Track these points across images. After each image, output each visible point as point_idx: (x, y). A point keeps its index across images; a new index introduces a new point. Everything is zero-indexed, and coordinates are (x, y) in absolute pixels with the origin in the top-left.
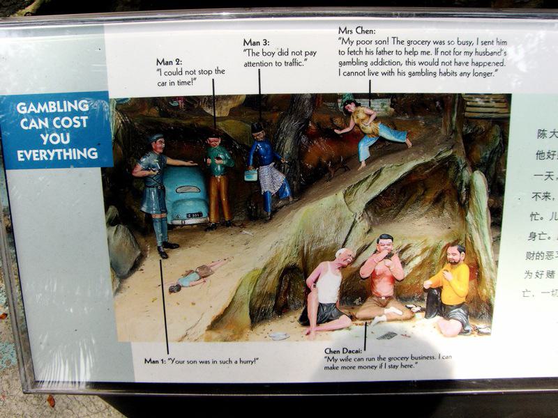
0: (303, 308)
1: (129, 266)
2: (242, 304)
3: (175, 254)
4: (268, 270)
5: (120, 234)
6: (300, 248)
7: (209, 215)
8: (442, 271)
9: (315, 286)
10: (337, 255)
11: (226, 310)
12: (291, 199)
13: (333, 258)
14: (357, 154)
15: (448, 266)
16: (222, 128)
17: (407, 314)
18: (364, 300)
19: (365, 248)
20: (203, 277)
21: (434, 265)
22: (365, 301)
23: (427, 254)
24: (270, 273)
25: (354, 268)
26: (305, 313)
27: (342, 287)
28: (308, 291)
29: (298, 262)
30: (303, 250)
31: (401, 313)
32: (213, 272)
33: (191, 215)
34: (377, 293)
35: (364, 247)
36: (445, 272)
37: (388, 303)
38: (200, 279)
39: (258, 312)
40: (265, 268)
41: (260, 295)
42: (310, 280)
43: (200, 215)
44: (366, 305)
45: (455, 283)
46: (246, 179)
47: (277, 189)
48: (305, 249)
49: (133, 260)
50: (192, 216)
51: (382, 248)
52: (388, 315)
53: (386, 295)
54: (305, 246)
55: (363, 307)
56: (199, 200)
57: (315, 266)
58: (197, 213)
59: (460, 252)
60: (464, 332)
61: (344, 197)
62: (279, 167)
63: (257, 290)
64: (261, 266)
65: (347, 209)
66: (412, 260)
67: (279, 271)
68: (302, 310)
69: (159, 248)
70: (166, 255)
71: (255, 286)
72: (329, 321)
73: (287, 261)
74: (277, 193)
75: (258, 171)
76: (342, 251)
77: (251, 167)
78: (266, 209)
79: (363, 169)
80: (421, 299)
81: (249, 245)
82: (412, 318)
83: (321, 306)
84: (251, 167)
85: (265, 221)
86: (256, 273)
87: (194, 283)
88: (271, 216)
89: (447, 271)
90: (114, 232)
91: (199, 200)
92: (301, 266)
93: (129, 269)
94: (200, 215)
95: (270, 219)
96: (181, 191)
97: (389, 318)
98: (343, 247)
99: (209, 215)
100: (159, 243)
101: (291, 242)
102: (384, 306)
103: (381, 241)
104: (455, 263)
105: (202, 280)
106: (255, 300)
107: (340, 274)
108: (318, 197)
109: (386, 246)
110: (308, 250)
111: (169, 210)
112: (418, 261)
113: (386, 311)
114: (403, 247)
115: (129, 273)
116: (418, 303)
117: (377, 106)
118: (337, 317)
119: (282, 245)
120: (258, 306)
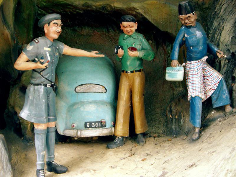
7: (114, 125)
16: (140, 11)
33: (91, 123)
43: (102, 125)
46: (168, 78)
47: (210, 94)
50: (91, 127)
56: (103, 103)
58: (98, 122)
62: (213, 62)
74: (209, 100)
75: (184, 67)
77: (175, 62)
78: (193, 119)
84: (175, 62)
91: (103, 103)
94: (102, 125)
95: (199, 138)
96: (82, 91)
99: (114, 125)
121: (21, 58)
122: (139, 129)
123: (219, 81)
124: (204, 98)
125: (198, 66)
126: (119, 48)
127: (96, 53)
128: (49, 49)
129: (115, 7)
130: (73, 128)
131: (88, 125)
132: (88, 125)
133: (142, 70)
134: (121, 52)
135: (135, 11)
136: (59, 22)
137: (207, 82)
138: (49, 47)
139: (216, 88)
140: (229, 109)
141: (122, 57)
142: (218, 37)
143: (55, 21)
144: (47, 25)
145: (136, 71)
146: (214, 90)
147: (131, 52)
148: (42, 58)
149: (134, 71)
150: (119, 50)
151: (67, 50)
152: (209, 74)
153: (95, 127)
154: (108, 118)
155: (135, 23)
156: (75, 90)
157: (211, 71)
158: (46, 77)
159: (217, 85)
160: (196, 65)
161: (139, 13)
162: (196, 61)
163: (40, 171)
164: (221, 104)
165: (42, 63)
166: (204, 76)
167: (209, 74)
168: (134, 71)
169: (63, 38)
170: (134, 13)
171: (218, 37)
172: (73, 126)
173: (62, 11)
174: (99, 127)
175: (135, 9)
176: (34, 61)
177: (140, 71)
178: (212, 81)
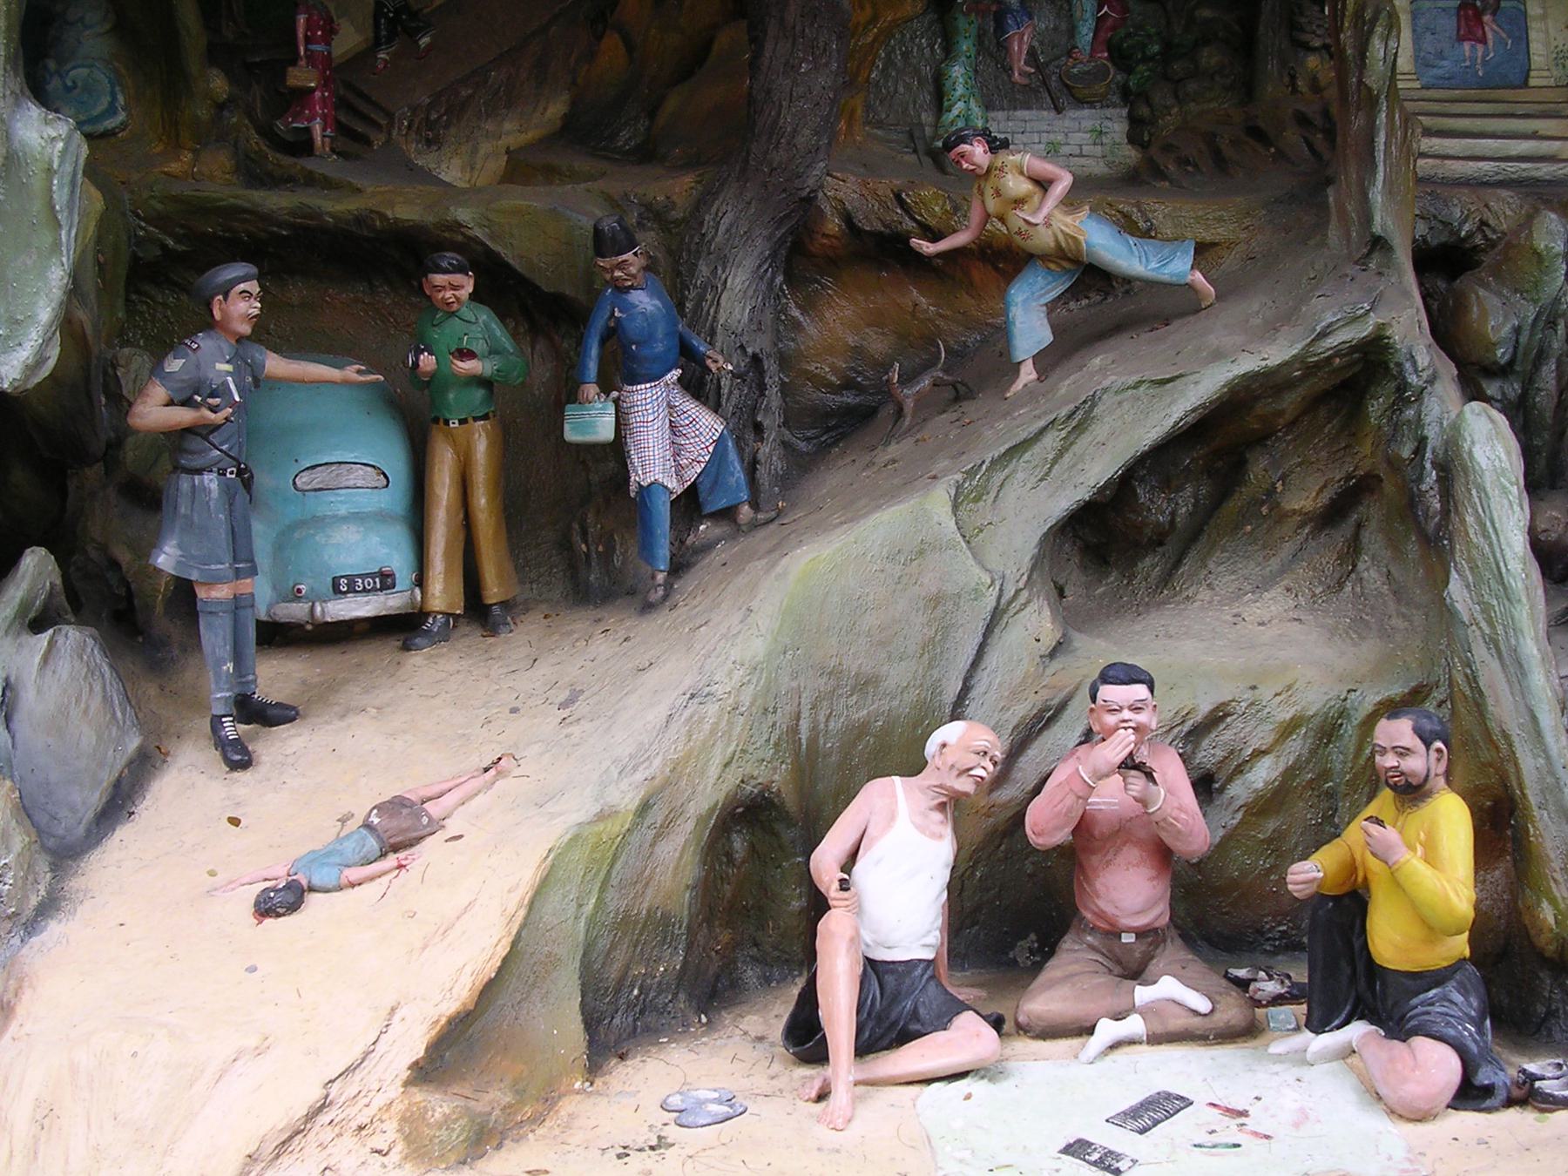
0: (801, 982)
1: (95, 799)
2: (552, 962)
3: (274, 746)
4: (657, 815)
5: (65, 666)
6: (782, 719)
7: (421, 581)
8: (1359, 823)
9: (844, 885)
10: (931, 746)
11: (489, 991)
12: (746, 511)
13: (913, 766)
14: (1001, 333)
15: (1384, 802)
16: (478, 233)
17: (1232, 1012)
18: (1047, 950)
19: (1045, 719)
20: (396, 848)
21: (1330, 795)
22: (1051, 953)
23: (1296, 746)
24: (662, 831)
25: (1004, 806)
26: (808, 1002)
27: (957, 886)
28: (819, 905)
29: (777, 776)
30: (794, 730)
31: (1201, 1004)
32: (436, 826)
33: (351, 580)
34: (1101, 915)
35: (1039, 716)
36: (1374, 829)
37: (1147, 959)
38: (383, 855)
39: (618, 991)
40: (645, 808)
41: (625, 922)
42: (826, 859)
43: (386, 581)
44: (1054, 969)
45: (1413, 864)
46: (571, 435)
47: (692, 474)
48: (804, 726)
49: (107, 777)
50: (352, 589)
51: (1111, 720)
52: (1147, 1012)
53: (1141, 921)
54: (805, 714)
55: (1043, 977)
56: (381, 517)
57: (844, 796)
58: (372, 575)
59: (1428, 745)
60: (1470, 1094)
61: (955, 507)
62: (698, 386)
63: (615, 902)
64: (626, 797)
65: (971, 561)
66: (1239, 770)
67: (702, 820)
68: (796, 991)
69: (216, 722)
70: (245, 751)
71: (602, 890)
72: (904, 1037)
73: (732, 779)
74: (692, 492)
75: (616, 401)
76: (951, 732)
77: (591, 390)
78: (647, 550)
79: (1030, 394)
80: (1290, 946)
81: (580, 707)
82: (1247, 1032)
83: (873, 968)
84: (591, 390)
85: (648, 608)
86: (615, 827)
87: (354, 874)
88: (668, 586)
89: (1380, 822)
90: (37, 659)
91: (381, 517)
92: (790, 801)
93: (90, 815)
94: (386, 581)
95: (666, 597)
96: (315, 485)
97: (1158, 1029)
98: (955, 716)
99: (421, 581)
100: (220, 696)
101: (746, 698)
102: (1136, 972)
103: (1109, 692)
104: (1412, 792)
105: (391, 860)
106: (603, 944)
107: (948, 831)
108: (852, 511)
109: (1126, 714)
110: (814, 728)
111: (263, 559)
112: (1263, 774)
113: (1143, 994)
114: (1199, 717)
115: (88, 831)
116: (1282, 963)
117: (1077, 138)
118: (942, 1021)
119: (712, 709)
120: (613, 973)
121: (148, 395)
122: (493, 591)
123: (715, 438)
124: (675, 486)
125: (655, 397)
126: (422, 352)
127: (359, 372)
128: (229, 368)
129: (396, 219)
130: (297, 596)
131: (342, 586)
132: (342, 586)
133: (491, 415)
134: (427, 361)
135: (462, 234)
136: (253, 287)
137: (683, 442)
138: (228, 362)
139: (707, 458)
140: (746, 511)
141: (431, 377)
142: (712, 311)
143: (242, 286)
144: (220, 297)
145: (475, 419)
146: (703, 465)
147: (460, 364)
148: (213, 395)
149: (470, 420)
150: (422, 357)
151: (275, 364)
152: (687, 418)
153: (365, 590)
154: (400, 562)
155: (467, 274)
156: (294, 483)
157: (693, 411)
158: (224, 447)
159: (711, 449)
160: (649, 395)
161: (475, 240)
162: (648, 385)
163: (224, 720)
164: (722, 503)
165: (214, 409)
166: (672, 426)
167: (687, 418)
168: (470, 420)
169: (265, 333)
170: (460, 238)
171: (712, 311)
172: (299, 591)
173: (220, 228)
174: (374, 590)
175: (461, 225)
176: (187, 403)
177: (485, 417)
178: (697, 439)
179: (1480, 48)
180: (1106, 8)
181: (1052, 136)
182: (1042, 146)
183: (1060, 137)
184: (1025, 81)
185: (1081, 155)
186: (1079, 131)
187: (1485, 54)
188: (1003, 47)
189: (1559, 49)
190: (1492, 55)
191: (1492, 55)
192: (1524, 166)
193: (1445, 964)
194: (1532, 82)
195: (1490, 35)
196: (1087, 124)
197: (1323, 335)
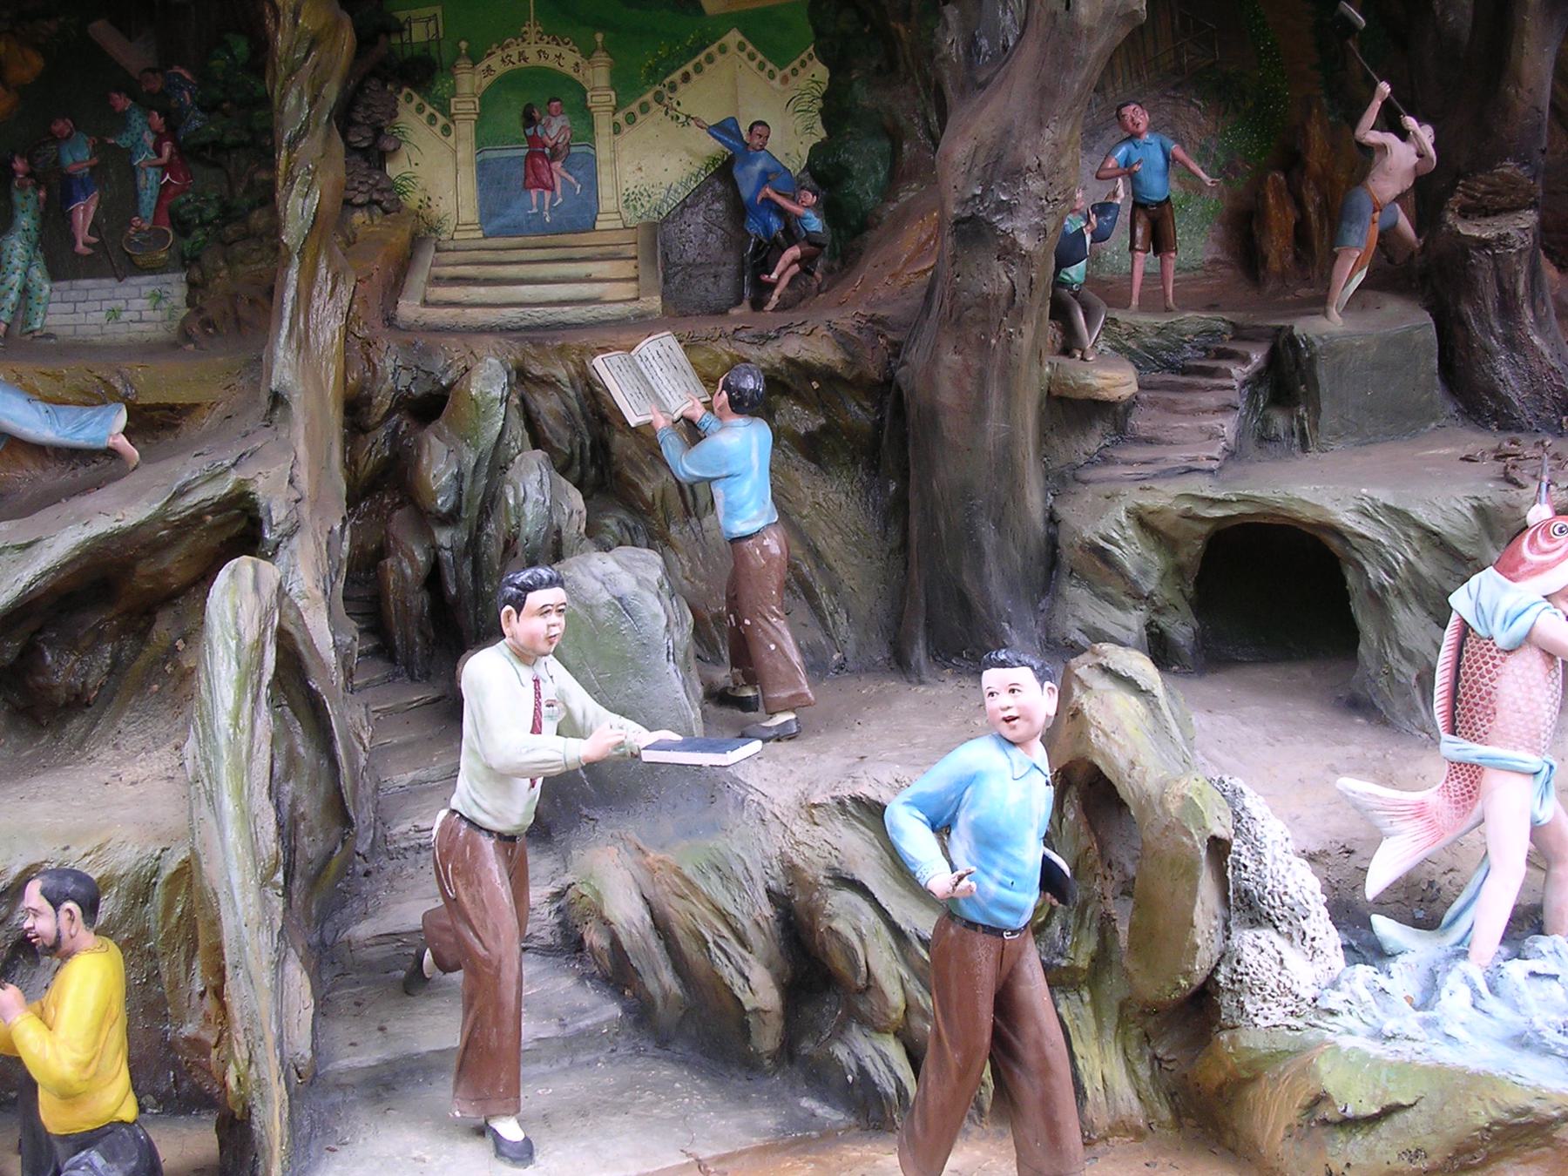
117: (138, 304)
179: (547, 194)
180: (168, 177)
181: (113, 304)
182: (104, 314)
183: (122, 304)
184: (89, 251)
185: (141, 321)
186: (140, 297)
187: (553, 200)
188: (67, 219)
189: (630, 191)
190: (560, 200)
191: (560, 200)
192: (549, 310)
193: (90, 1127)
194: (599, 226)
195: (558, 181)
196: (147, 290)
197: (181, 493)
